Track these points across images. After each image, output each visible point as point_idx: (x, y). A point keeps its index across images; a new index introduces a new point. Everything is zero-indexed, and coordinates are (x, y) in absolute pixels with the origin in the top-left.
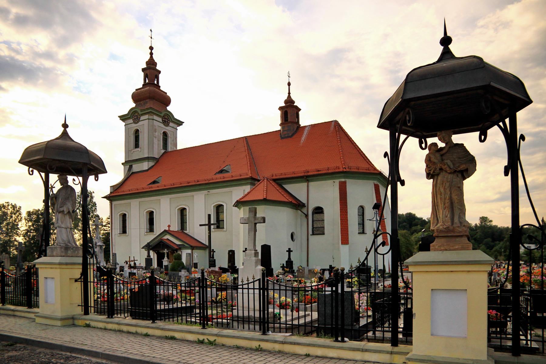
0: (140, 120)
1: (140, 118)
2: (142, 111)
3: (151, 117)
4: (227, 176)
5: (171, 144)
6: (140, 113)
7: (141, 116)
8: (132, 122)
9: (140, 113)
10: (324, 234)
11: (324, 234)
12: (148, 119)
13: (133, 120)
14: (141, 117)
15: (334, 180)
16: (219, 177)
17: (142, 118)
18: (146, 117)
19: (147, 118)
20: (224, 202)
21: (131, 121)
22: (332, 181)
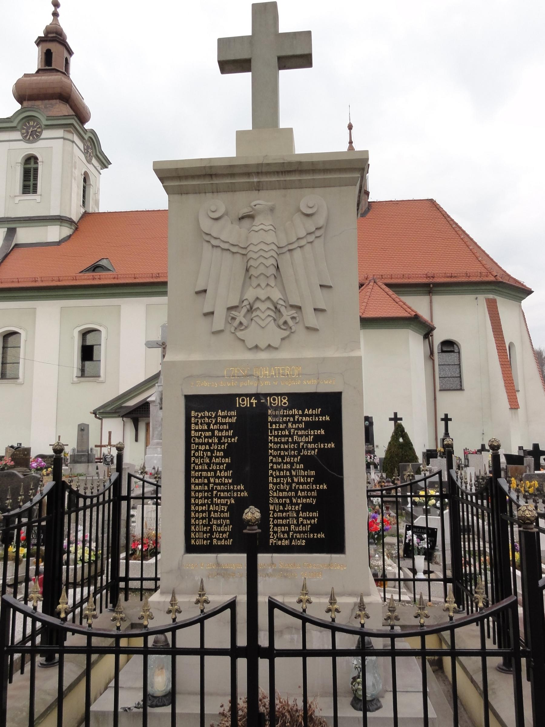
0: (42, 137)
1: (41, 133)
2: (49, 118)
3: (69, 136)
4: (104, 278)
5: (93, 199)
6: (44, 122)
7: (45, 129)
8: (21, 138)
9: (44, 122)
10: (461, 389)
11: (461, 389)
12: (64, 139)
13: (22, 134)
14: (43, 131)
15: (477, 296)
16: (88, 279)
17: (46, 134)
18: (60, 133)
19: (62, 136)
20: (105, 327)
21: (17, 135)
22: (474, 296)
